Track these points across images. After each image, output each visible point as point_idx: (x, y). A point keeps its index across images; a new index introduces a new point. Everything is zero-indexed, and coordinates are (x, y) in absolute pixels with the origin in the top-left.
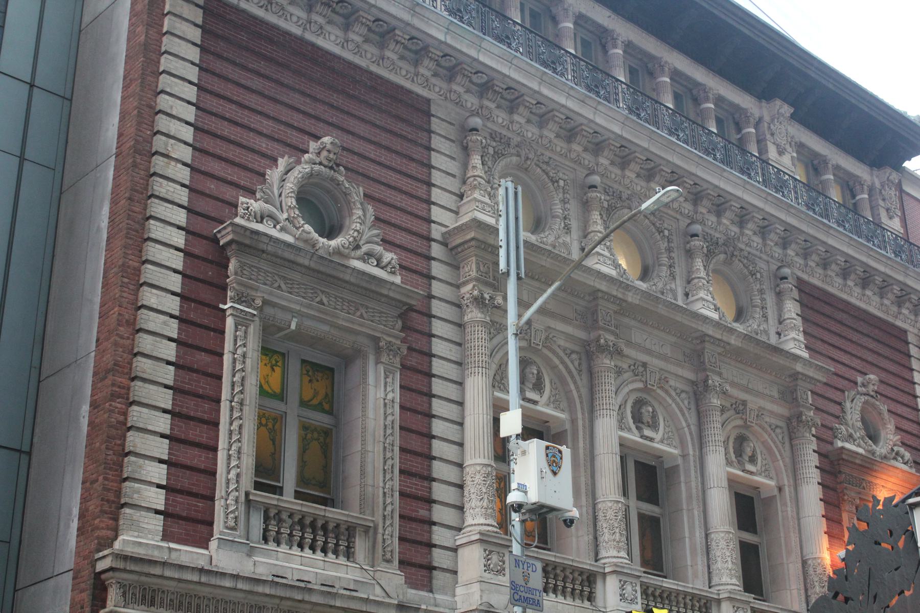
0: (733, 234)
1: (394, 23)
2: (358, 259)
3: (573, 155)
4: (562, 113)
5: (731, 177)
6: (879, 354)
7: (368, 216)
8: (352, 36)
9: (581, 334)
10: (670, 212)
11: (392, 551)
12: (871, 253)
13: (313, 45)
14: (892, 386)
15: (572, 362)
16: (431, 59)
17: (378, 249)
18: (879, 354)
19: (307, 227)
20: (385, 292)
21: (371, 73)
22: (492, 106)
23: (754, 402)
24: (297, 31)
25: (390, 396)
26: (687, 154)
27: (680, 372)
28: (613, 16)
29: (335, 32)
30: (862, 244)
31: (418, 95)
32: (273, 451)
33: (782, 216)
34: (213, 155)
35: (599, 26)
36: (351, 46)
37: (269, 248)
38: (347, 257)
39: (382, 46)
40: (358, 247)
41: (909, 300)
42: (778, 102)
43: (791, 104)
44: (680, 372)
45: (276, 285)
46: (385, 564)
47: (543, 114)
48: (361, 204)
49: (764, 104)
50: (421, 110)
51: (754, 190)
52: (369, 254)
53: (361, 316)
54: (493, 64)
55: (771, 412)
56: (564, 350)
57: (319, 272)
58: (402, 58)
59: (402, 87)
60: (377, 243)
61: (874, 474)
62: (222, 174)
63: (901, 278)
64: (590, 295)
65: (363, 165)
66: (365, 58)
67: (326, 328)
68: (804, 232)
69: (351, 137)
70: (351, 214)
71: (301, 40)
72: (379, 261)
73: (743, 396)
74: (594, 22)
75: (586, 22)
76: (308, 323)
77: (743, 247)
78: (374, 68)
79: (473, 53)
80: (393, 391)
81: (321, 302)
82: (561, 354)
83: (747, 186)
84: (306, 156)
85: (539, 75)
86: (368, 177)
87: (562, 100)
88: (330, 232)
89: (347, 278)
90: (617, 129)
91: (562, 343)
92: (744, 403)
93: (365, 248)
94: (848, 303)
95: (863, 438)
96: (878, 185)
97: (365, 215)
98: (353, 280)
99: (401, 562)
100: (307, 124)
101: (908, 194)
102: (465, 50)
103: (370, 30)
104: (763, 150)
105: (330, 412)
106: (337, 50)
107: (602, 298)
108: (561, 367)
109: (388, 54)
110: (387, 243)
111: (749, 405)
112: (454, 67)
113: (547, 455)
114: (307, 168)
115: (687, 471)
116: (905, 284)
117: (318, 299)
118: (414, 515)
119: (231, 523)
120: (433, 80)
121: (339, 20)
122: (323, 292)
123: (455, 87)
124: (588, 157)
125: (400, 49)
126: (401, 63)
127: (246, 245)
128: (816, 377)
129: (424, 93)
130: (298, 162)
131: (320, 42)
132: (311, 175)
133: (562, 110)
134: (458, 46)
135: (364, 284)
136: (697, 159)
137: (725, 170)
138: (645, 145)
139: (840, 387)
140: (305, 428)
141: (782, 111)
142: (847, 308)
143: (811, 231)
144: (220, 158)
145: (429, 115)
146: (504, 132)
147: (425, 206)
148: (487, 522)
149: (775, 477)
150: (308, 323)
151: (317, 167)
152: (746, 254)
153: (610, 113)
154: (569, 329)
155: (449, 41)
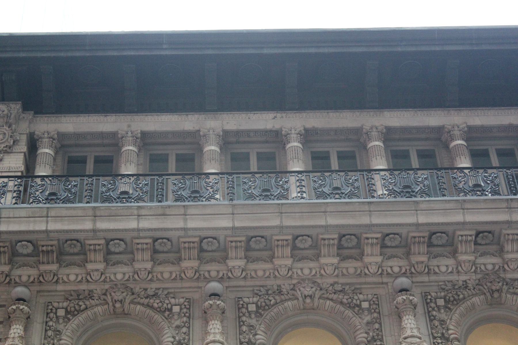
0: (490, 267)
4: (145, 238)
5: (432, 205)
22: (54, 267)
26: (347, 208)
28: (279, 115)
35: (266, 132)
51: (483, 205)
74: (256, 132)
75: (249, 136)
85: (90, 213)
87: (133, 224)
121: (400, 252)
123: (137, 266)
124: (396, 264)
136: (366, 208)
137: (417, 202)
138: (276, 222)
146: (84, 287)
153: (208, 211)
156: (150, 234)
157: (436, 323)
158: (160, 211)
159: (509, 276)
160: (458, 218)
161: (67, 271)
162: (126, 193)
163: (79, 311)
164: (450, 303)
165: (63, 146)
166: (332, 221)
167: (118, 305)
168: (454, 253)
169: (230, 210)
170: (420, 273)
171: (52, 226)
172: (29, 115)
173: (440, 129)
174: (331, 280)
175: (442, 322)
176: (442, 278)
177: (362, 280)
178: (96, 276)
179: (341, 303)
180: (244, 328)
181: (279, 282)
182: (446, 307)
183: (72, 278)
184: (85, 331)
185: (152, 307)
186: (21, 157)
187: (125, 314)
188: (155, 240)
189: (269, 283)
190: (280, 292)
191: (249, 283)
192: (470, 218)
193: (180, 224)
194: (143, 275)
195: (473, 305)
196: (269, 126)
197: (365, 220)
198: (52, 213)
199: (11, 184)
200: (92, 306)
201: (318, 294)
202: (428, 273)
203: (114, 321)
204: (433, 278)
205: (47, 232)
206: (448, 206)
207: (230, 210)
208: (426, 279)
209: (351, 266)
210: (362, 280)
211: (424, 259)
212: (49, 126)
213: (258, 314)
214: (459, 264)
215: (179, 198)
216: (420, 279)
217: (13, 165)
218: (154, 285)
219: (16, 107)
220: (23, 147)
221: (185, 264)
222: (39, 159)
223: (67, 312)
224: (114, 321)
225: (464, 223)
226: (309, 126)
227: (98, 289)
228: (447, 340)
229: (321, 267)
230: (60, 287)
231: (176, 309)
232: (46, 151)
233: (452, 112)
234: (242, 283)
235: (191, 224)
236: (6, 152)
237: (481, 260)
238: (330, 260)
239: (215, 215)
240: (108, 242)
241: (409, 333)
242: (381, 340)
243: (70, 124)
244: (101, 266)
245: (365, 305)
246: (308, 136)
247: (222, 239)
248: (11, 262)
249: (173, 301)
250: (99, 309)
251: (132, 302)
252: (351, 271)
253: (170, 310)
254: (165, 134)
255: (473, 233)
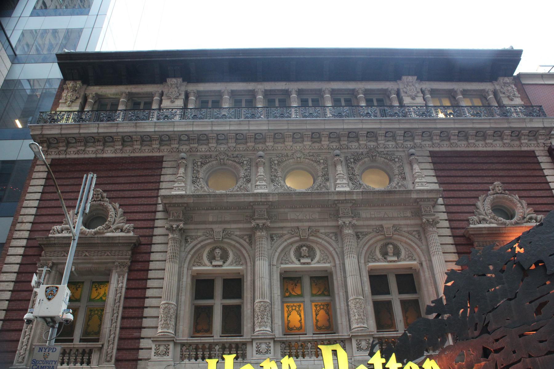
0: (372, 146)
1: (519, 130)
2: (527, 222)
3: (251, 148)
6: (509, 170)
7: (524, 205)
8: (505, 141)
9: (418, 222)
10: (324, 151)
11: (111, 356)
12: (474, 121)
13: (102, 158)
14: (525, 183)
15: (245, 241)
16: (525, 135)
17: (534, 215)
18: (509, 170)
19: (500, 218)
20: (117, 241)
21: (132, 157)
22: (196, 145)
23: (387, 224)
24: (93, 156)
25: (120, 285)
27: (326, 224)
29: (499, 143)
30: (388, 119)
31: (157, 156)
32: (100, 323)
33: (397, 126)
34: (136, 212)
35: (282, 90)
36: (436, 145)
37: (56, 242)
38: (103, 233)
39: (519, 139)
40: (524, 218)
41: (522, 135)
42: (404, 78)
43: (79, 80)
44: (326, 224)
45: (63, 255)
46: (107, 363)
47: (221, 138)
48: (519, 201)
49: (399, 82)
50: (532, 155)
51: (370, 121)
52: (116, 229)
53: (108, 255)
54: (183, 129)
55: (407, 225)
56: (408, 232)
57: (83, 244)
58: (529, 140)
59: (148, 157)
60: (532, 214)
61: (505, 235)
62: (48, 221)
63: (506, 126)
64: (415, 202)
65: (513, 187)
66: (127, 153)
67: (90, 265)
68: (418, 128)
69: (117, 185)
70: (517, 207)
71: (97, 158)
72: (536, 220)
73: (378, 223)
74: (278, 90)
76: (81, 266)
77: (383, 150)
78: (132, 155)
79: (171, 129)
80: (122, 283)
81: (86, 256)
82: (237, 239)
83: (364, 121)
84: (489, 192)
86: (118, 198)
87: (227, 128)
88: (511, 217)
89: (96, 242)
90: (265, 127)
91: (238, 233)
92: (382, 226)
93: (528, 217)
94: (478, 151)
95: (494, 218)
96: (498, 87)
97: (522, 205)
98: (99, 242)
99: (117, 360)
100: (486, 180)
101: (524, 84)
102: (166, 130)
103: (511, 136)
104: (400, 100)
105: (329, 295)
106: (113, 155)
107: (421, 201)
108: (237, 245)
109: (523, 141)
110: (128, 221)
111: (384, 227)
112: (518, 135)
113: (46, 291)
114: (492, 197)
115: (336, 272)
116: (511, 128)
117: (84, 255)
118: (130, 336)
119: (108, 359)
120: (512, 143)
122: (86, 251)
123: (230, 145)
125: (526, 137)
126: (530, 142)
127: (46, 244)
128: (431, 196)
129: (161, 154)
130: (487, 196)
131: (105, 155)
132: (494, 199)
133: (231, 132)
134: (162, 130)
135: (105, 242)
136: (323, 122)
137: (343, 120)
138: (286, 127)
139: (475, 196)
140: (403, 303)
141: (408, 80)
142: (477, 154)
143: (422, 126)
144: (140, 212)
145: (536, 157)
146: (208, 153)
147: (549, 191)
148: (359, 326)
149: (417, 259)
150: (81, 266)
151: (495, 196)
152: (385, 152)
153: (258, 123)
154: (241, 226)
155: (157, 129)
156: (235, 132)
157: (350, 168)
158: (239, 123)
159: (380, 150)
160: (360, 126)
161: (201, 147)
162: (224, 115)
163: (206, 163)
164: (356, 161)
165: (199, 96)
166: (309, 127)
167: (222, 161)
168: (358, 141)
169: (267, 122)
170: (344, 149)
171: (195, 129)
172: (185, 83)
173: (353, 90)
174: (308, 151)
175: (352, 168)
176: (353, 151)
177: (320, 151)
178: (213, 149)
179: (312, 160)
180: (273, 170)
181: (287, 152)
182: (354, 162)
183: (203, 150)
184: (209, 171)
185: (235, 161)
186: (182, 100)
187: (225, 164)
188: (237, 134)
189: (283, 152)
190: (287, 156)
191: (275, 152)
192: (365, 126)
193: (247, 128)
194: (232, 149)
195: (365, 161)
196: (284, 88)
197: (322, 127)
198: (195, 123)
199: (178, 111)
200: (211, 161)
201: (303, 157)
202: (348, 148)
203: (220, 167)
204: (349, 150)
205: (193, 131)
206: (356, 121)
207: (267, 122)
208: (346, 151)
209: (317, 145)
210: (320, 151)
211: (346, 143)
212: (193, 88)
213: (278, 164)
214: (360, 145)
215: (247, 117)
216: (344, 151)
217: (179, 104)
218: (236, 153)
219: (180, 80)
220: (183, 96)
221: (249, 144)
222: (189, 101)
223: (201, 163)
224: (220, 167)
225: (362, 128)
226: (300, 88)
227: (214, 154)
228: (354, 175)
229: (304, 146)
230: (198, 153)
231: (245, 162)
232: (192, 98)
233: (359, 83)
234: (272, 152)
235: (251, 128)
236: (176, 99)
237: (369, 144)
238: (308, 143)
239: (261, 124)
240: (217, 135)
241: (339, 172)
242: (328, 175)
243: (203, 87)
244: (215, 145)
245: (322, 161)
246: (300, 92)
247: (264, 134)
248: (179, 143)
249: (244, 159)
250: (214, 162)
251: (227, 159)
252: (316, 147)
253: (243, 163)
254: (240, 91)
255: (366, 132)
